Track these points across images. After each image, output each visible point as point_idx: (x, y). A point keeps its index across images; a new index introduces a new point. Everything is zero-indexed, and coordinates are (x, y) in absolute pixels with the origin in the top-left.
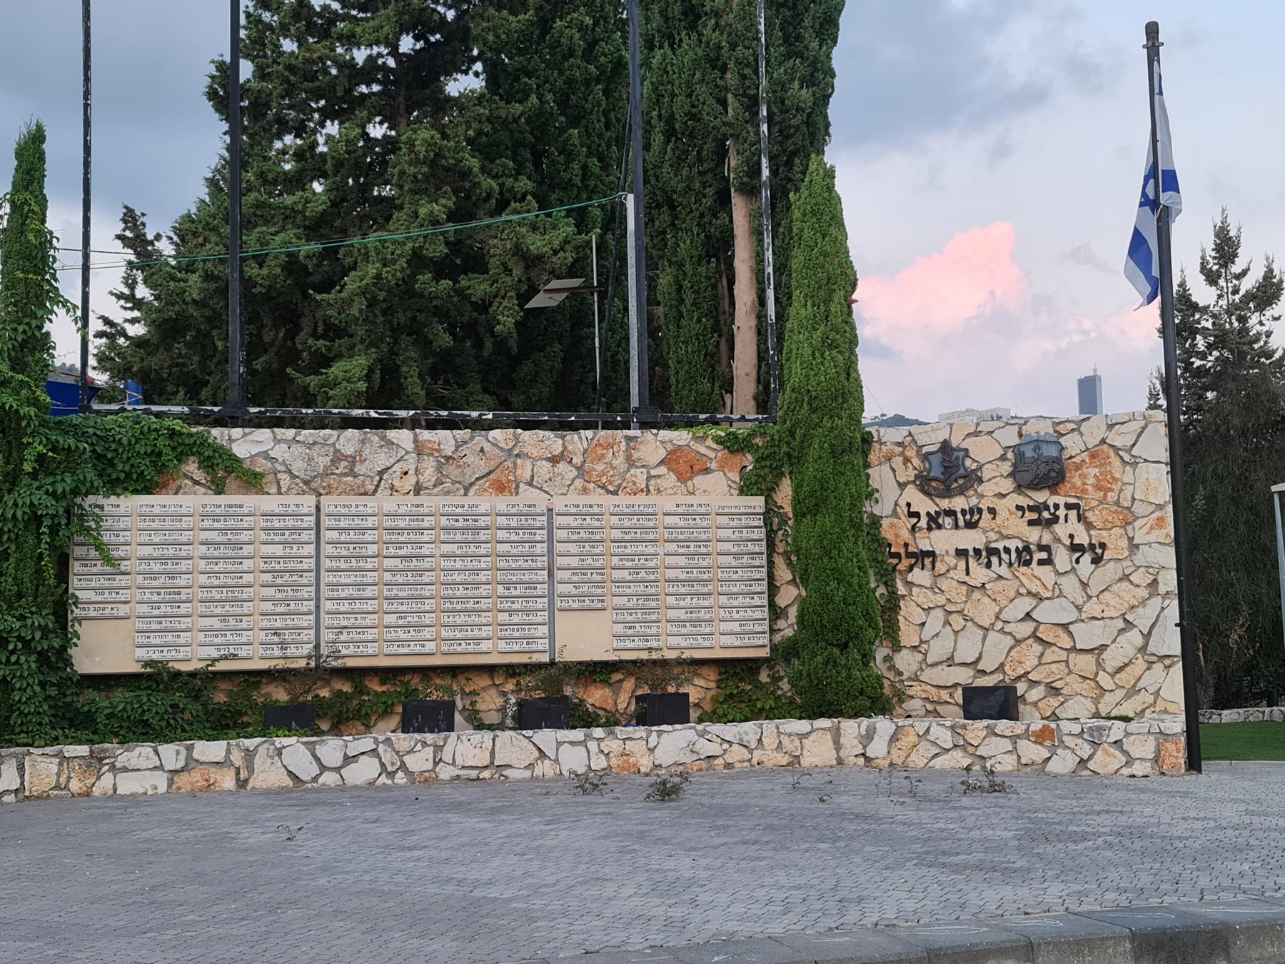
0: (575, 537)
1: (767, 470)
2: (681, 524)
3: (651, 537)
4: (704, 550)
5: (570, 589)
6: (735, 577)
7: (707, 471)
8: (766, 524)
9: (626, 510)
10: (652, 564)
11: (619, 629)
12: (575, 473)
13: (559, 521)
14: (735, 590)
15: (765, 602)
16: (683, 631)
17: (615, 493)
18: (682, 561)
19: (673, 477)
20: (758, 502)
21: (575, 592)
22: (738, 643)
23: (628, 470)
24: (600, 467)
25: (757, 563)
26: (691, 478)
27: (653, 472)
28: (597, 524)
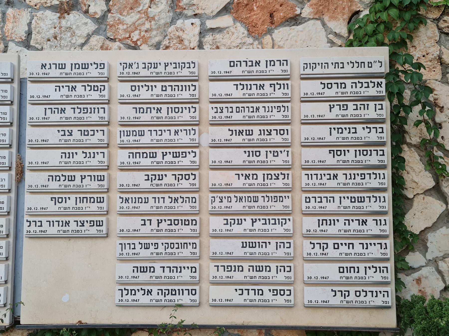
0: (55, 117)
1: (394, 12)
2: (238, 94)
3: (186, 116)
4: (277, 139)
5: (44, 201)
6: (332, 184)
7: (295, 20)
8: (390, 95)
9: (144, 73)
10: (186, 162)
11: (126, 270)
12: (92, 27)
13: (32, 90)
14: (331, 207)
15: (389, 229)
16: (238, 276)
17: (135, 47)
18: (238, 157)
19: (241, 30)
20: (377, 56)
21: (52, 207)
22: (337, 301)
23: (173, 22)
24: (131, 18)
25: (374, 160)
26: (269, 32)
27: (210, 24)
28: (95, 95)
